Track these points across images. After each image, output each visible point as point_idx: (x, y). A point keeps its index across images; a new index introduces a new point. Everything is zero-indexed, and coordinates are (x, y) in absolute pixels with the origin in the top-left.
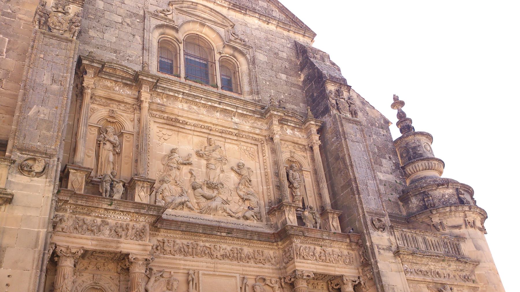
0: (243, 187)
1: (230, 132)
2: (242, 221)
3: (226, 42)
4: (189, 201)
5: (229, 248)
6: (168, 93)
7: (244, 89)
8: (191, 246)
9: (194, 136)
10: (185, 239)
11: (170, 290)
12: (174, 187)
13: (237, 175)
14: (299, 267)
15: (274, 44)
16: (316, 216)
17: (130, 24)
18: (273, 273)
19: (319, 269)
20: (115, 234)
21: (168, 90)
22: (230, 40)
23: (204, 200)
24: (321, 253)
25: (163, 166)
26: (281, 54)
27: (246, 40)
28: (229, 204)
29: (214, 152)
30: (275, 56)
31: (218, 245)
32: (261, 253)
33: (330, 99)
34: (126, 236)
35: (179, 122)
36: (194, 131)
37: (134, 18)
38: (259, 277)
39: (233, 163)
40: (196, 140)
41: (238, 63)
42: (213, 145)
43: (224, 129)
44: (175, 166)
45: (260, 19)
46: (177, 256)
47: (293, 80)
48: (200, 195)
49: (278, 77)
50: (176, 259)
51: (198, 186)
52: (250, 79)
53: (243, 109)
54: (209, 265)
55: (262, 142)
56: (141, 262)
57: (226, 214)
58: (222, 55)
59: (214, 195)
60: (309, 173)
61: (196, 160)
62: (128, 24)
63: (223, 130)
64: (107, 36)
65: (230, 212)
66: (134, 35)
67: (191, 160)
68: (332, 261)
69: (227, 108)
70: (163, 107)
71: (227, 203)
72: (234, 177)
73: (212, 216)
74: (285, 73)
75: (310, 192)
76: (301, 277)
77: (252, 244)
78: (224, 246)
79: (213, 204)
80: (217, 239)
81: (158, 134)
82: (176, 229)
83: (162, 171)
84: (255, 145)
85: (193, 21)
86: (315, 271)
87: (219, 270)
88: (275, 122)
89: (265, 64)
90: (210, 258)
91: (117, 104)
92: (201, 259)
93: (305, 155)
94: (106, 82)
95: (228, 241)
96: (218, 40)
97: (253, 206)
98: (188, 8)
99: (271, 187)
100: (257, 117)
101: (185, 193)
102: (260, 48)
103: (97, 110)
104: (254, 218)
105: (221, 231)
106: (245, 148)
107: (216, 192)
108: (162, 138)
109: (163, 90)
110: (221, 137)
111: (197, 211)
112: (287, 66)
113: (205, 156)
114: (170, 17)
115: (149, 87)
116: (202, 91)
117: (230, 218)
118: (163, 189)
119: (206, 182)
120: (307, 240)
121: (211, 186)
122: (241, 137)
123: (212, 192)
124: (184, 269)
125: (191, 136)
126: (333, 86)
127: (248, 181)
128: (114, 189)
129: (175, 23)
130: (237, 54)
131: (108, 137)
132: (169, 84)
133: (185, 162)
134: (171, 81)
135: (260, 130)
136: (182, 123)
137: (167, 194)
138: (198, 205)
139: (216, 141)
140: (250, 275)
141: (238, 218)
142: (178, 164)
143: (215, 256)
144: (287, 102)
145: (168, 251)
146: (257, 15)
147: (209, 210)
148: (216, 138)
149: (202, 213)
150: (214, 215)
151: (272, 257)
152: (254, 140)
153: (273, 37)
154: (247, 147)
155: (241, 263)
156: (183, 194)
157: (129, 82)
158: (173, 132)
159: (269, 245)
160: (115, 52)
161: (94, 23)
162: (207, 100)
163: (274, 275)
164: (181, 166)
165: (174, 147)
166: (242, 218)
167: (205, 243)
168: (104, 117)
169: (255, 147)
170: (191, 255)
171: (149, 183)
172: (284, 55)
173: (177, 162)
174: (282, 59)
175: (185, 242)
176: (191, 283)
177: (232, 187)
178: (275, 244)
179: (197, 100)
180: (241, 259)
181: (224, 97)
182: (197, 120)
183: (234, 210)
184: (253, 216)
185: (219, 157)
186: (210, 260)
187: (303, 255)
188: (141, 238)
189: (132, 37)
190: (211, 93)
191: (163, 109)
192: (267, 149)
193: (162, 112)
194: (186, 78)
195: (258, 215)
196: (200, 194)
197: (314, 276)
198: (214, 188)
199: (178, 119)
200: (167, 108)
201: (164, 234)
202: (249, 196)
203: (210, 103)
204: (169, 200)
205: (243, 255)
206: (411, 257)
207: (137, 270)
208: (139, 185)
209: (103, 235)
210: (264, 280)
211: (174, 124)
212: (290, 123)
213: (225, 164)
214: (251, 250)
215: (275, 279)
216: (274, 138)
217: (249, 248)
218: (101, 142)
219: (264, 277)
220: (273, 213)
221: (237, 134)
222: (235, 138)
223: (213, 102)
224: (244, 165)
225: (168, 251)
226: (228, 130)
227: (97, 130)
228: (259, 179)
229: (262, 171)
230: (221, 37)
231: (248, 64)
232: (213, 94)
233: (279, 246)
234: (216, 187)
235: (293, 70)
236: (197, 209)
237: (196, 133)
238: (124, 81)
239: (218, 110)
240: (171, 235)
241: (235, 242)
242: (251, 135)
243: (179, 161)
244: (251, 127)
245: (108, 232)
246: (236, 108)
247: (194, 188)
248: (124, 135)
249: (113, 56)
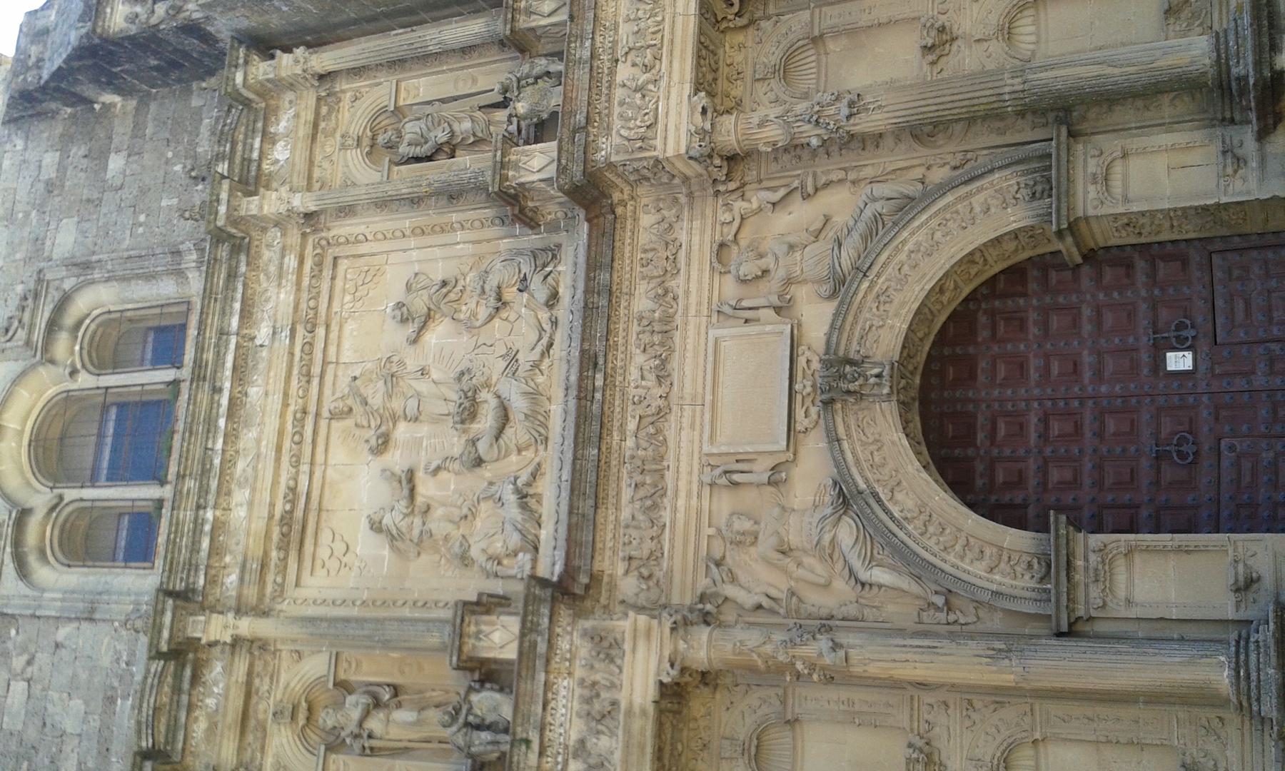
0: (464, 308)
1: (302, 351)
2: (562, 312)
3: (35, 356)
4: (516, 478)
5: (639, 359)
6: (204, 554)
7: (172, 295)
8: (638, 478)
9: (331, 461)
10: (618, 494)
11: (756, 538)
12: (478, 523)
13: (431, 325)
14: (678, 143)
15: (22, 195)
16: (528, 77)
18: (703, 215)
19: (682, 70)
20: (607, 721)
21: (194, 554)
22: (28, 343)
23: (509, 432)
24: (634, 65)
25: (423, 556)
26: (49, 172)
27: (20, 289)
28: (518, 351)
29: (370, 401)
30: (56, 192)
31: (632, 391)
32: (650, 255)
33: (153, 21)
34: (613, 686)
35: (291, 512)
36: (312, 463)
38: (716, 265)
39: (397, 335)
40: (338, 454)
41: (96, 313)
42: (350, 402)
43: (295, 371)
44: (417, 521)
46: (666, 516)
47: (121, 130)
48: (495, 447)
49: (119, 183)
50: (673, 523)
51: (470, 453)
52: (138, 277)
53: (228, 311)
54: (686, 422)
55: (324, 243)
56: (682, 645)
57: (546, 363)
58: (79, 366)
59: (493, 402)
60: (403, 85)
61: (398, 453)
63: (300, 373)
65: (539, 349)
67: (397, 470)
68: (659, 23)
69: (229, 364)
70: (248, 566)
71: (514, 359)
73: (553, 407)
75: (461, 84)
76: (707, 138)
77: (624, 287)
78: (634, 374)
79: (518, 404)
80: (614, 399)
81: (333, 573)
82: (591, 527)
83: (437, 557)
84: (335, 265)
86: (688, 88)
87: (700, 390)
88: (251, 206)
89: (86, 225)
90: (668, 416)
91: (254, 699)
92: (671, 444)
93: (349, 95)
94: (194, 735)
95: (619, 364)
96: (34, 380)
97: (516, 277)
99: (455, 217)
100: (248, 264)
101: (494, 488)
102: (38, 242)
103: (277, 756)
104: (551, 272)
105: (590, 388)
106: (348, 298)
107: (484, 395)
108: (344, 560)
109: (197, 570)
110: (322, 377)
111: (541, 452)
112: (83, 151)
113: (383, 428)
115: (191, 619)
116: (190, 436)
117: (556, 351)
118: (485, 559)
119: (458, 426)
120: (599, 113)
121: (469, 411)
122: (316, 314)
123: (486, 406)
124: (699, 496)
125: (330, 472)
126: (112, 9)
127: (444, 290)
128: (489, 720)
129: (4, 521)
130: (69, 319)
131: (352, 727)
132: (181, 540)
133: (406, 492)
134: (172, 536)
135: (288, 252)
136: (293, 502)
137: (499, 545)
138: (527, 448)
139: (338, 395)
140: (711, 291)
141: (555, 323)
142: (413, 511)
143: (661, 402)
144: (192, 153)
145: (653, 545)
147: (537, 418)
148: (327, 391)
149: (547, 439)
150: (549, 399)
151: (658, 217)
152: (321, 271)
154: (344, 290)
155: (678, 320)
156: (498, 496)
157: (188, 672)
158: (323, 524)
159: (623, 229)
162: (213, 430)
163: (709, 212)
164: (419, 500)
165: (364, 523)
166: (554, 312)
167: (628, 433)
168: (296, 738)
169: (343, 265)
170: (662, 477)
171: (467, 619)
172: (51, 159)
173: (406, 515)
174: (61, 168)
175: (627, 494)
176: (736, 477)
177: (466, 340)
178: (619, 210)
179: (217, 461)
180: (667, 319)
181: (200, 367)
182: (278, 459)
184: (546, 277)
185: (381, 383)
186: (672, 418)
187: (642, 130)
188: (617, 644)
189: (63, 653)
190: (194, 411)
191: (254, 566)
192: (343, 229)
193: (264, 566)
194: (163, 483)
195: (542, 262)
196: (491, 445)
197: (703, 94)
198: (474, 399)
199: (282, 518)
200: (250, 554)
201: (606, 558)
202: (487, 288)
203: (222, 422)
204: (515, 540)
205: (657, 315)
207: (702, 654)
208: (474, 647)
209: (612, 753)
210: (722, 245)
211: (297, 527)
212: (251, 150)
213: (401, 363)
214: (642, 287)
215: (720, 212)
216: (302, 210)
217: (637, 292)
218: (366, 745)
219: (715, 247)
220: (530, 214)
221: (309, 326)
222: (321, 331)
223: (218, 413)
224: (400, 305)
225: (653, 545)
226: (297, 358)
227: (334, 756)
228: (438, 252)
229: (413, 242)
230: (23, 374)
231: (93, 282)
232: (195, 404)
233: (626, 197)
234: (470, 394)
235: (93, 129)
236: (537, 450)
237: (320, 458)
238: (186, 686)
239: (240, 392)
240: (608, 538)
241: (621, 341)
242: (306, 282)
243: (405, 511)
244: (279, 285)
245: (604, 742)
246: (225, 337)
247: (479, 462)
248: (342, 676)
249: (124, 707)
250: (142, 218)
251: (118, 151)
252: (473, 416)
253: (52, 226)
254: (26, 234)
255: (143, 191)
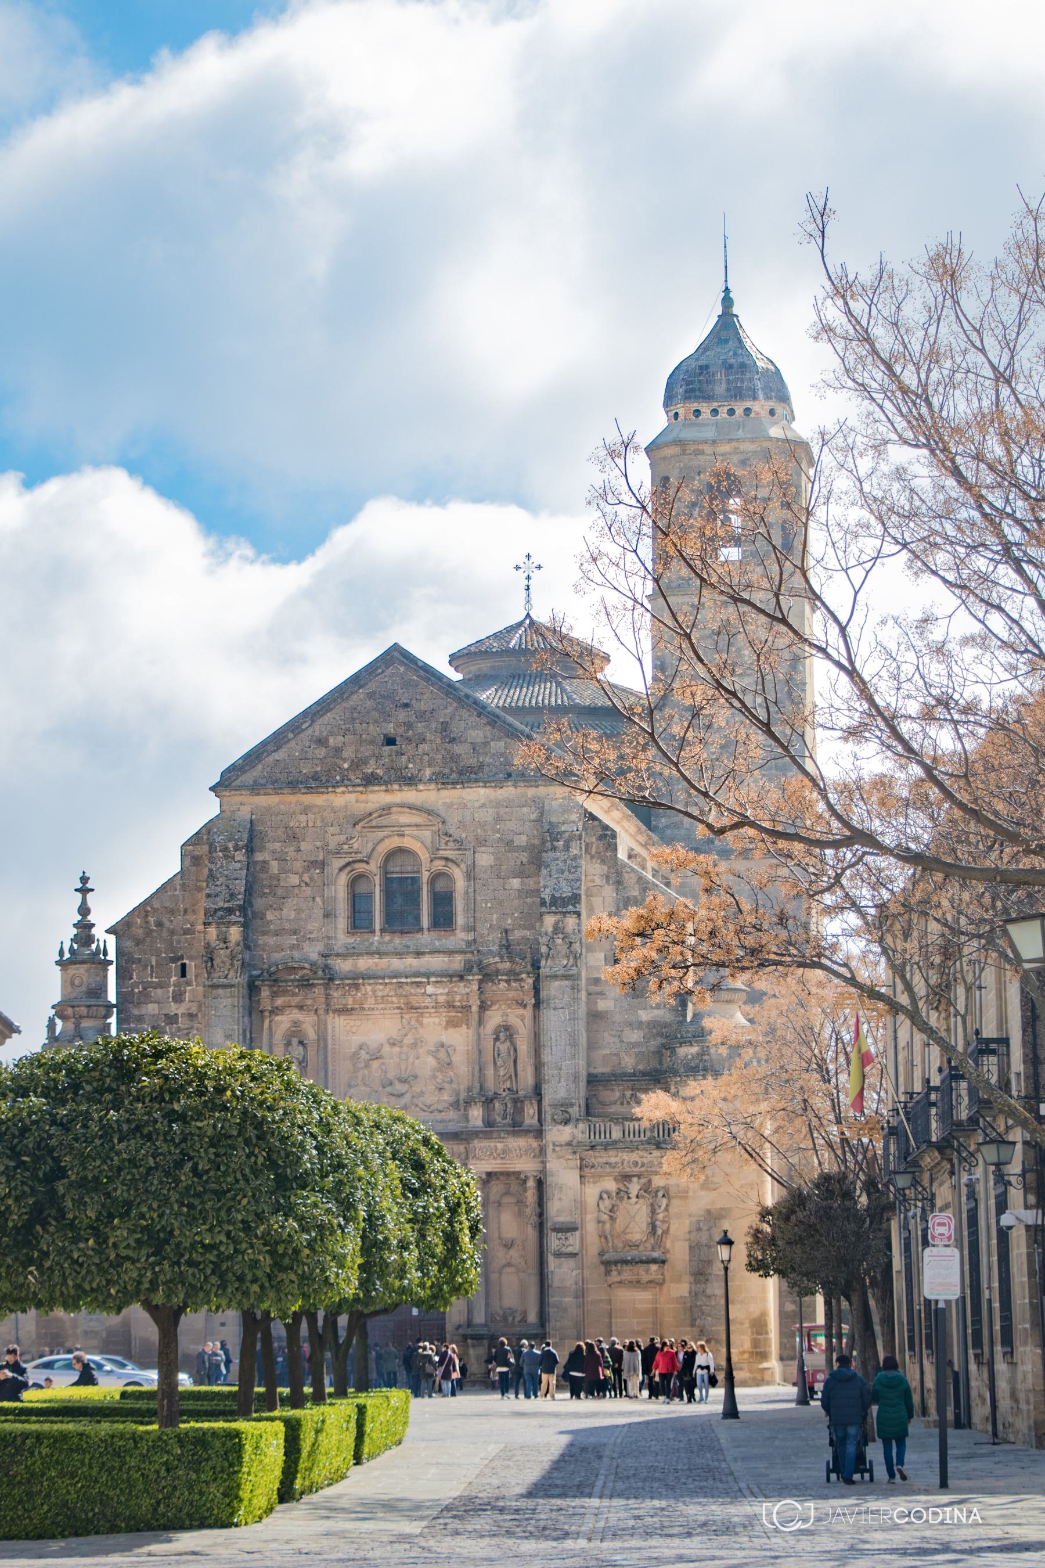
17: (307, 880)
23: (393, 1098)
27: (464, 835)
37: (312, 871)
44: (363, 1065)
45: (485, 787)
62: (306, 884)
64: (285, 912)
66: (314, 898)
72: (431, 1061)
74: (521, 874)
85: (388, 837)
98: (380, 816)
107: (407, 1086)
112: (525, 860)
114: (355, 846)
121: (403, 1081)
130: (450, 864)
146: (481, 784)
153: (507, 810)
160: (295, 933)
161: (271, 900)
172: (522, 840)
183: (428, 1102)
185: (412, 1041)
194: (382, 931)
203: (395, 981)
206: (591, 1152)
222: (433, 1010)
224: (443, 1046)
250: (489, 905)
251: (522, 883)
252: (403, 1081)
253: (491, 850)
254: (489, 833)
255: (501, 903)
